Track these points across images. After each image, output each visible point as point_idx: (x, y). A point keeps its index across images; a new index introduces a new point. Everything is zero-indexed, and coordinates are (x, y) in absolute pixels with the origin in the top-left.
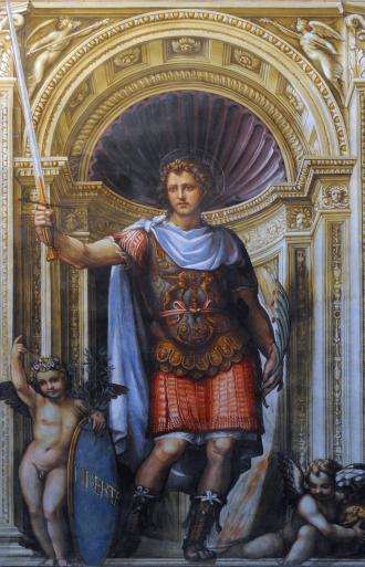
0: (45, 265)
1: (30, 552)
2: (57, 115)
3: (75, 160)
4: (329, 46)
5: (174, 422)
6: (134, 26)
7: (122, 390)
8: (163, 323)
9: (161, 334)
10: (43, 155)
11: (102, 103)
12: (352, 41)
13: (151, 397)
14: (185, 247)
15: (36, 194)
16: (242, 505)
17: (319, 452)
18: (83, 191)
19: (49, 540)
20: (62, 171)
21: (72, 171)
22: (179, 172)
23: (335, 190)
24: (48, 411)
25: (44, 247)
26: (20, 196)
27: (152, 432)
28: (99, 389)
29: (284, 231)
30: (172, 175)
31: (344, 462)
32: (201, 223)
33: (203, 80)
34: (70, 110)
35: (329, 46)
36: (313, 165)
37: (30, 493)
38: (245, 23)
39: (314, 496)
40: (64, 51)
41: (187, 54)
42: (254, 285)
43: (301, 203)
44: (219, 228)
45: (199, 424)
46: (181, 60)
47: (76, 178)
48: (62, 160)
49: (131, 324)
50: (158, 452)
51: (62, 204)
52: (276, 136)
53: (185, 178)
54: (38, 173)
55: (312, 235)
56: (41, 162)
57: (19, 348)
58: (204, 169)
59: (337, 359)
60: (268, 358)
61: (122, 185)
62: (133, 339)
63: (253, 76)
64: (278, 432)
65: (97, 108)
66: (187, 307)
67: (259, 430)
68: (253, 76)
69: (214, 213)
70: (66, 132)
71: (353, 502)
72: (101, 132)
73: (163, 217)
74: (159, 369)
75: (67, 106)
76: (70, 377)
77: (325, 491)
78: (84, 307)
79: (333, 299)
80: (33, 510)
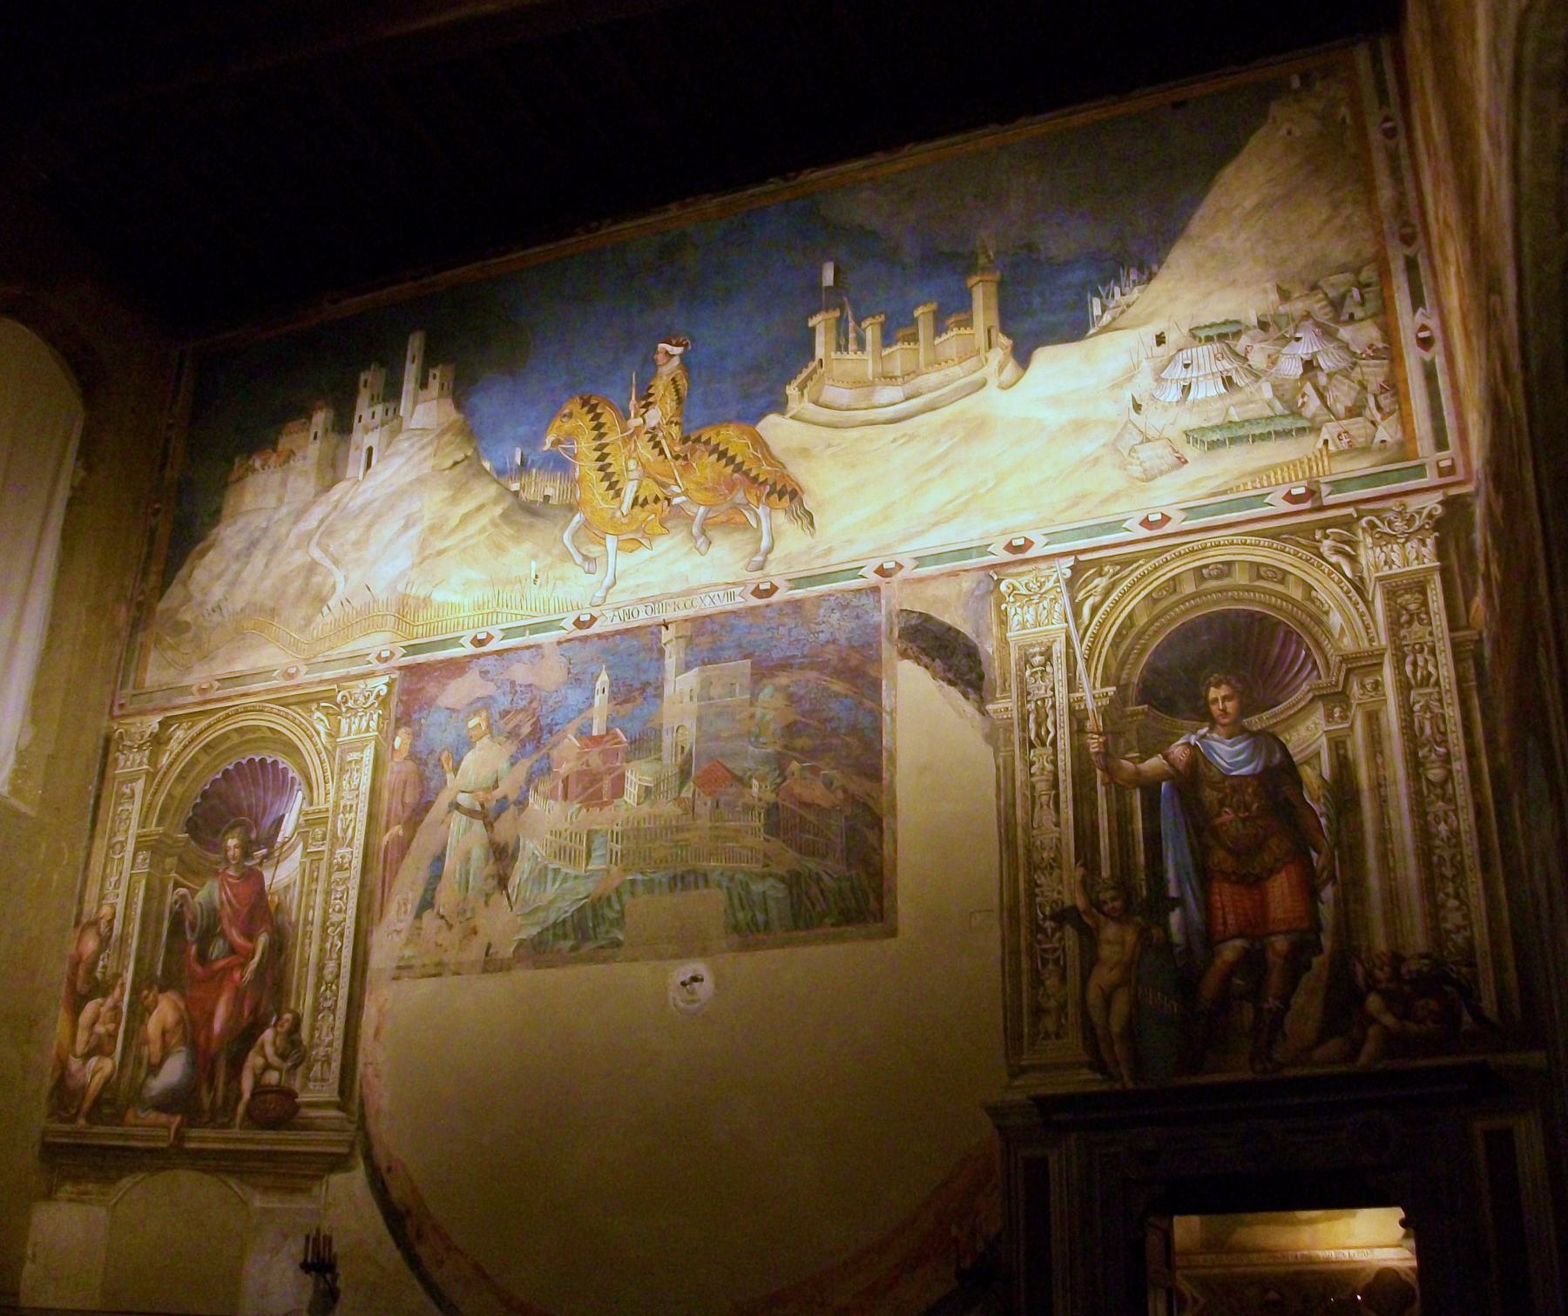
0: (1101, 790)
1: (1099, 1076)
2: (1104, 651)
3: (1122, 688)
7: (1179, 902)
9: (1212, 842)
12: (1369, 540)
13: (1207, 907)
14: (1227, 754)
15: (1089, 725)
16: (1307, 1007)
17: (1381, 944)
22: (1217, 686)
23: (1369, 681)
24: (1110, 931)
25: (1099, 772)
27: (1210, 940)
29: (1323, 726)
34: (1115, 644)
36: (1345, 659)
37: (1096, 1016)
38: (1267, 541)
39: (1379, 992)
40: (1107, 593)
41: (1217, 578)
42: (1298, 782)
43: (1336, 698)
44: (1260, 732)
45: (1255, 928)
46: (1213, 584)
47: (1125, 704)
48: (1111, 690)
50: (1218, 962)
51: (1112, 732)
53: (1223, 691)
55: (1351, 727)
56: (1093, 694)
57: (1080, 872)
66: (1235, 812)
67: (1317, 928)
69: (1255, 719)
70: (1114, 665)
77: (1390, 986)
78: (1139, 824)
79: (1379, 785)
80: (1099, 1032)
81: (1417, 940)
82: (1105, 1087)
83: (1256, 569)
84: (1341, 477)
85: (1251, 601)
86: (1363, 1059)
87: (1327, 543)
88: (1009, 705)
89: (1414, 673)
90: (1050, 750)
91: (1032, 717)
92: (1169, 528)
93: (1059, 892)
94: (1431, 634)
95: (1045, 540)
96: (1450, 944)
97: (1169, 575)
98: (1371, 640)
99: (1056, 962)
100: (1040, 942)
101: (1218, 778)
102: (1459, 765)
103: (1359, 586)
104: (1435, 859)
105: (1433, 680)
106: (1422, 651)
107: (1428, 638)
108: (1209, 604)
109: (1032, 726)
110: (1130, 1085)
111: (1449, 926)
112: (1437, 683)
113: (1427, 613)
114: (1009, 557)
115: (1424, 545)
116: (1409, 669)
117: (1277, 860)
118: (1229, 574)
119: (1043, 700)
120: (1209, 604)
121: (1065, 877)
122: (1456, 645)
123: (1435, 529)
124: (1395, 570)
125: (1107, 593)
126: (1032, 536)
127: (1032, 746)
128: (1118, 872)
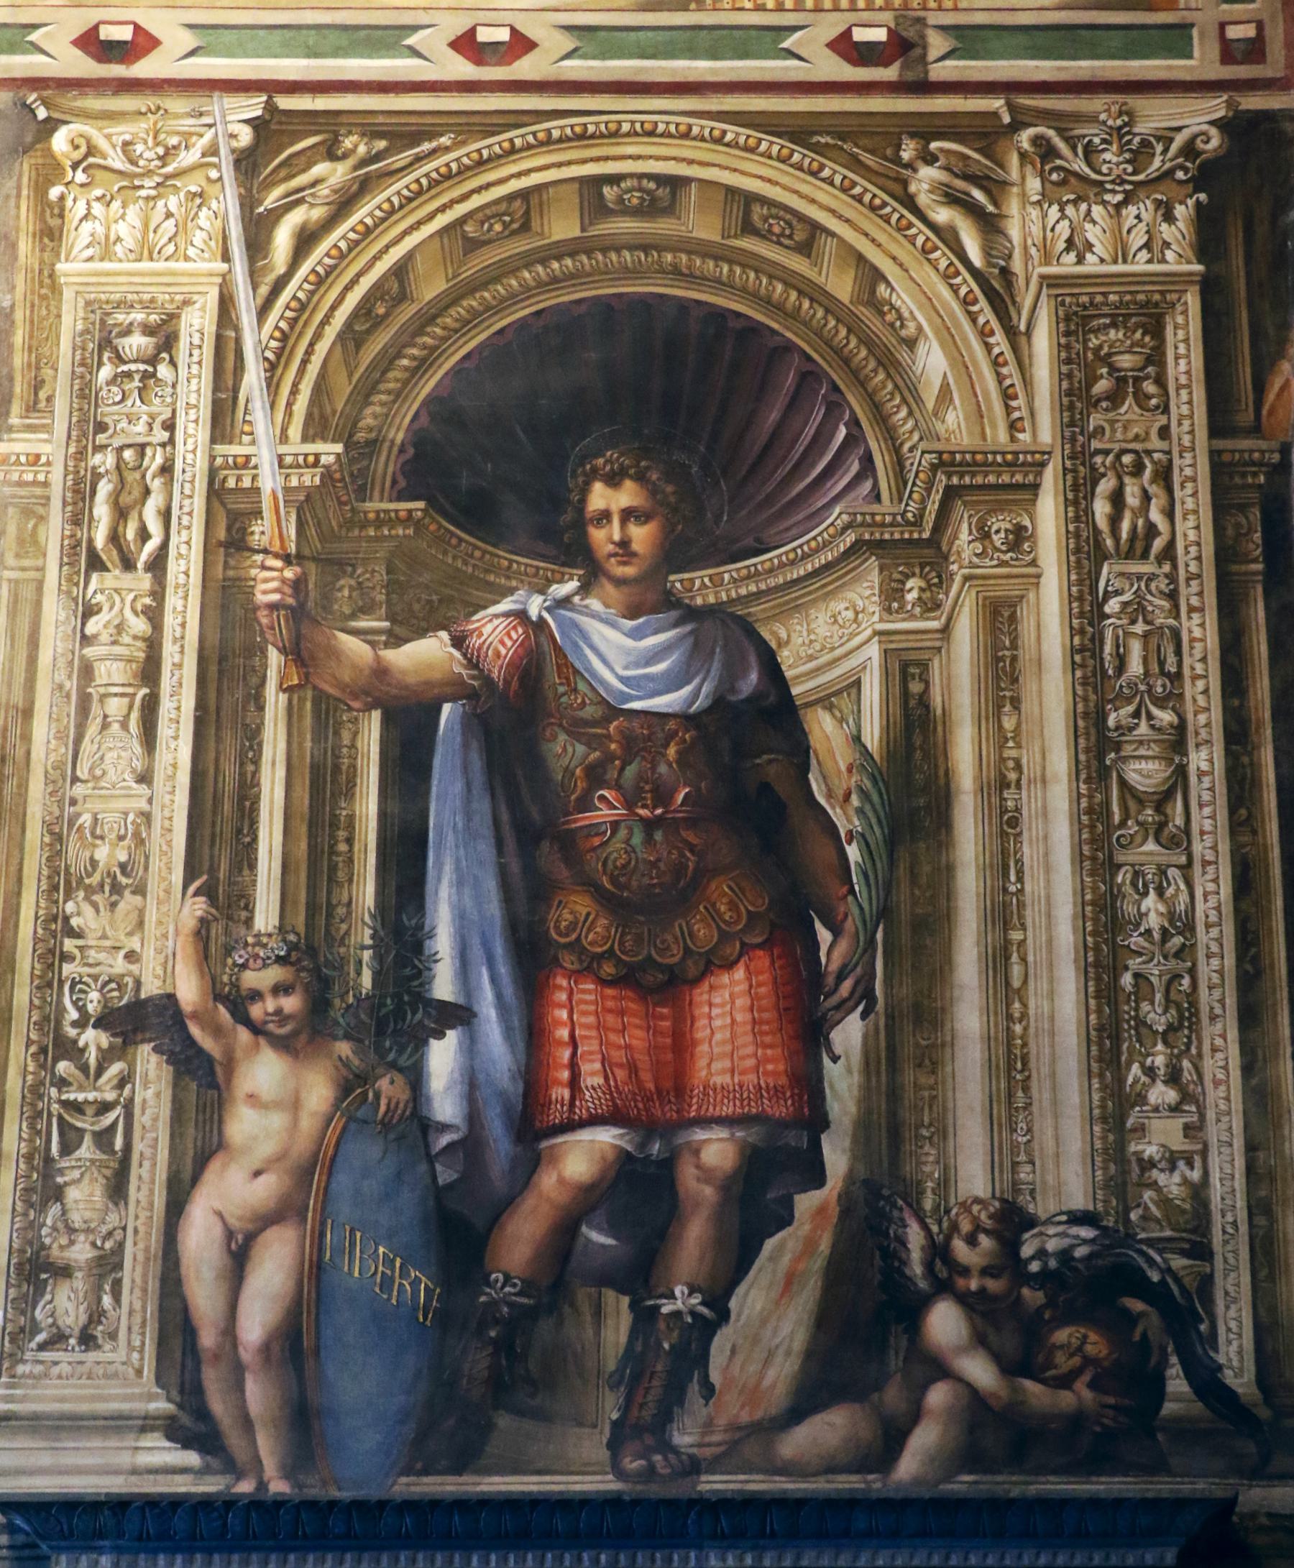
1: (192, 1458)
2: (322, 348)
3: (361, 451)
4: (978, 195)
5: (591, 1101)
6: (513, 150)
7: (458, 1016)
8: (568, 844)
10: (284, 438)
11: (432, 320)
12: (1034, 184)
13: (533, 1036)
14: (622, 655)
15: (261, 531)
16: (770, 1326)
17: (975, 1179)
18: (379, 523)
19: (247, 1424)
20: (327, 475)
21: (350, 480)
22: (613, 480)
23: (1000, 524)
24: (263, 1072)
26: (221, 534)
27: (534, 1126)
28: (399, 1013)
29: (874, 620)
30: (598, 487)
31: (1042, 1207)
32: (668, 601)
33: (676, 271)
34: (352, 338)
35: (978, 195)
36: (945, 462)
37: (203, 1294)
38: (776, 145)
39: (964, 1300)
40: (344, 204)
41: (637, 212)
42: (799, 752)
43: (913, 555)
45: (656, 1106)
47: (362, 493)
48: (330, 451)
49: (486, 848)
50: (547, 1181)
52: (854, 401)
53: (627, 496)
54: (269, 481)
55: (946, 630)
56: (276, 452)
57: (198, 907)
58: (675, 473)
59: (1016, 936)
60: (837, 932)
61: (476, 513)
62: (491, 885)
63: (797, 263)
64: (864, 1126)
65: (420, 331)
66: (629, 805)
68: (797, 263)
69: (701, 576)
70: (343, 388)
71: (1064, 1319)
72: (428, 385)
73: (572, 585)
74: (556, 961)
75: (349, 325)
76: (326, 983)
77: (993, 1285)
78: (368, 805)
79: (1000, 783)
80: (208, 1339)
81: (1067, 1178)
82: (211, 1486)
83: (743, 208)
84: (980, 18)
85: (719, 284)
86: (908, 1466)
87: (928, 174)
88: (46, 449)
89: (1115, 521)
90: (144, 581)
91: (104, 488)
92: (525, 68)
93: (131, 956)
94: (1164, 432)
95: (189, 40)
96: (1148, 1195)
97: (515, 185)
98: (1013, 426)
99: (103, 1138)
100: (62, 1083)
101: (590, 712)
102: (1206, 760)
103: (998, 290)
104: (1127, 980)
105: (1158, 544)
106: (1138, 469)
107: (1155, 443)
108: (605, 273)
109: (102, 510)
110: (278, 1487)
111: (1151, 1151)
112: (1169, 553)
113: (1160, 381)
114: (84, 66)
115: (1169, 218)
116: (1101, 509)
117: (724, 937)
118: (670, 210)
119: (141, 448)
120: (605, 273)
121: (152, 916)
122: (1220, 468)
123: (1199, 182)
124: (1092, 265)
125: (344, 204)
126: (154, 23)
127: (96, 563)
128: (300, 921)
